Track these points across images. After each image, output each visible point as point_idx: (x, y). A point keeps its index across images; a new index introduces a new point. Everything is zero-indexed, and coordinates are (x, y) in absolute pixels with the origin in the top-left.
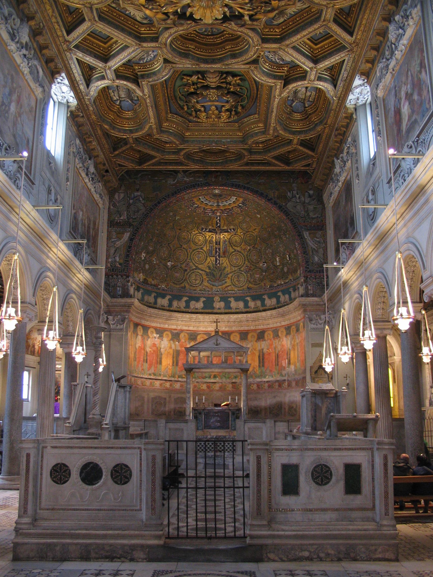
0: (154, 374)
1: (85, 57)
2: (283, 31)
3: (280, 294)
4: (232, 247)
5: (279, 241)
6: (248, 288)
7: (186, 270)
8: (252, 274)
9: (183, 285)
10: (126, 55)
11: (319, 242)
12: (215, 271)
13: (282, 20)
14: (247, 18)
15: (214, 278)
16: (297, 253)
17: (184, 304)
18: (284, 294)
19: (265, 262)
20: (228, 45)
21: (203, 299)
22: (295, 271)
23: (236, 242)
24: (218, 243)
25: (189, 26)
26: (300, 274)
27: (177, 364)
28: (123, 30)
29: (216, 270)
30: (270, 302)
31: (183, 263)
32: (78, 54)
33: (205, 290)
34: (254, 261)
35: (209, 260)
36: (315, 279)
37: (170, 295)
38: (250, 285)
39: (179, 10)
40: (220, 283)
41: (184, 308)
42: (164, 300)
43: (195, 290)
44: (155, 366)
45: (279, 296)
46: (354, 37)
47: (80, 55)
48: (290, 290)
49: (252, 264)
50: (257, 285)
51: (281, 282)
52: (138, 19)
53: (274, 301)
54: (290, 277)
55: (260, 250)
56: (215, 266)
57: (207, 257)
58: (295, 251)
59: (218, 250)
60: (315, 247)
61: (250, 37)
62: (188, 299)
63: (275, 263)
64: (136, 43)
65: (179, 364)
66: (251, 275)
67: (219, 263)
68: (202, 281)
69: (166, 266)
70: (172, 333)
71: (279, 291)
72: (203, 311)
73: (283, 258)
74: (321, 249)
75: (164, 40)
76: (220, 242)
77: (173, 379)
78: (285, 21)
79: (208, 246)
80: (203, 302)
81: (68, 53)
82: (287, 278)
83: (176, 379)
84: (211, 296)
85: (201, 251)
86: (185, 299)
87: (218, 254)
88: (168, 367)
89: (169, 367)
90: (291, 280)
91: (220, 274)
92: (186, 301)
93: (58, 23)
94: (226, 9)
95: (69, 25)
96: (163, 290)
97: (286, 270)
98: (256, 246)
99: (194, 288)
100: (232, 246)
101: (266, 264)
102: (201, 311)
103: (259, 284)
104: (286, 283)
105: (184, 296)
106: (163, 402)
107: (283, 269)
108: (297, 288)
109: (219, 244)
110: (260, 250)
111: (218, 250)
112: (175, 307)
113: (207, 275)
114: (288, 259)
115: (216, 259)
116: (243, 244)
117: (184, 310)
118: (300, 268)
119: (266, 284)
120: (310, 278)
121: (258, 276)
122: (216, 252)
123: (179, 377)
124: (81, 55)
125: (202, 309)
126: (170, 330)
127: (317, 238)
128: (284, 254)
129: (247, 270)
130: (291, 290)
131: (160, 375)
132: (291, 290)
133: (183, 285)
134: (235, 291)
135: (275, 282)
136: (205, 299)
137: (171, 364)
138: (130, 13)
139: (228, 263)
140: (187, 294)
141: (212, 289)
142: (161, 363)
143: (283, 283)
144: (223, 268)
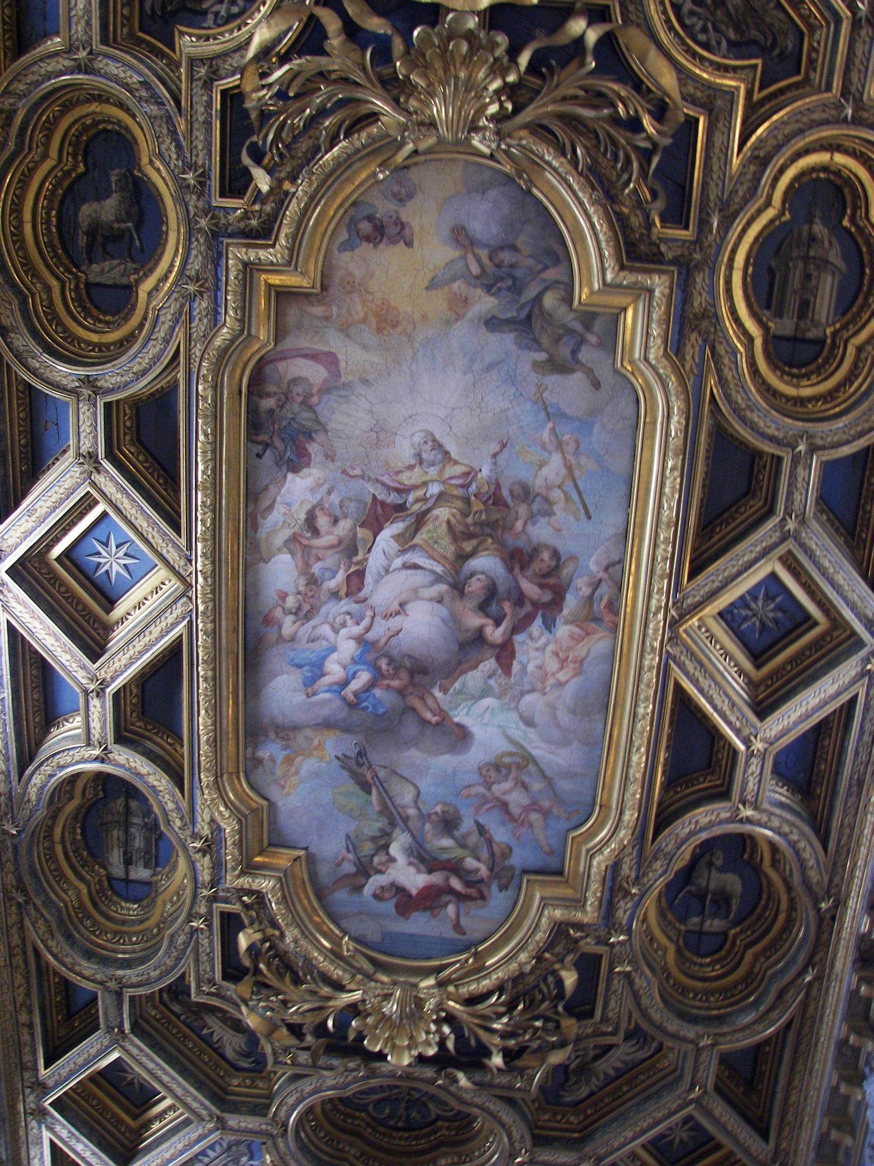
1: (73, 1142)
2: (587, 1121)
10: (180, 1146)
13: (584, 1092)
14: (497, 1060)
20: (445, 1155)
25: (350, 1078)
28: (184, 1072)
32: (58, 1128)
39: (330, 1023)
46: (772, 1143)
47: (64, 1130)
52: (229, 1053)
61: (503, 1125)
64: (211, 1116)
75: (282, 1113)
78: (592, 1094)
81: (34, 1124)
93: (31, 1026)
94: (446, 1029)
95: (57, 1043)
124: (64, 1134)
138: (213, 1032)
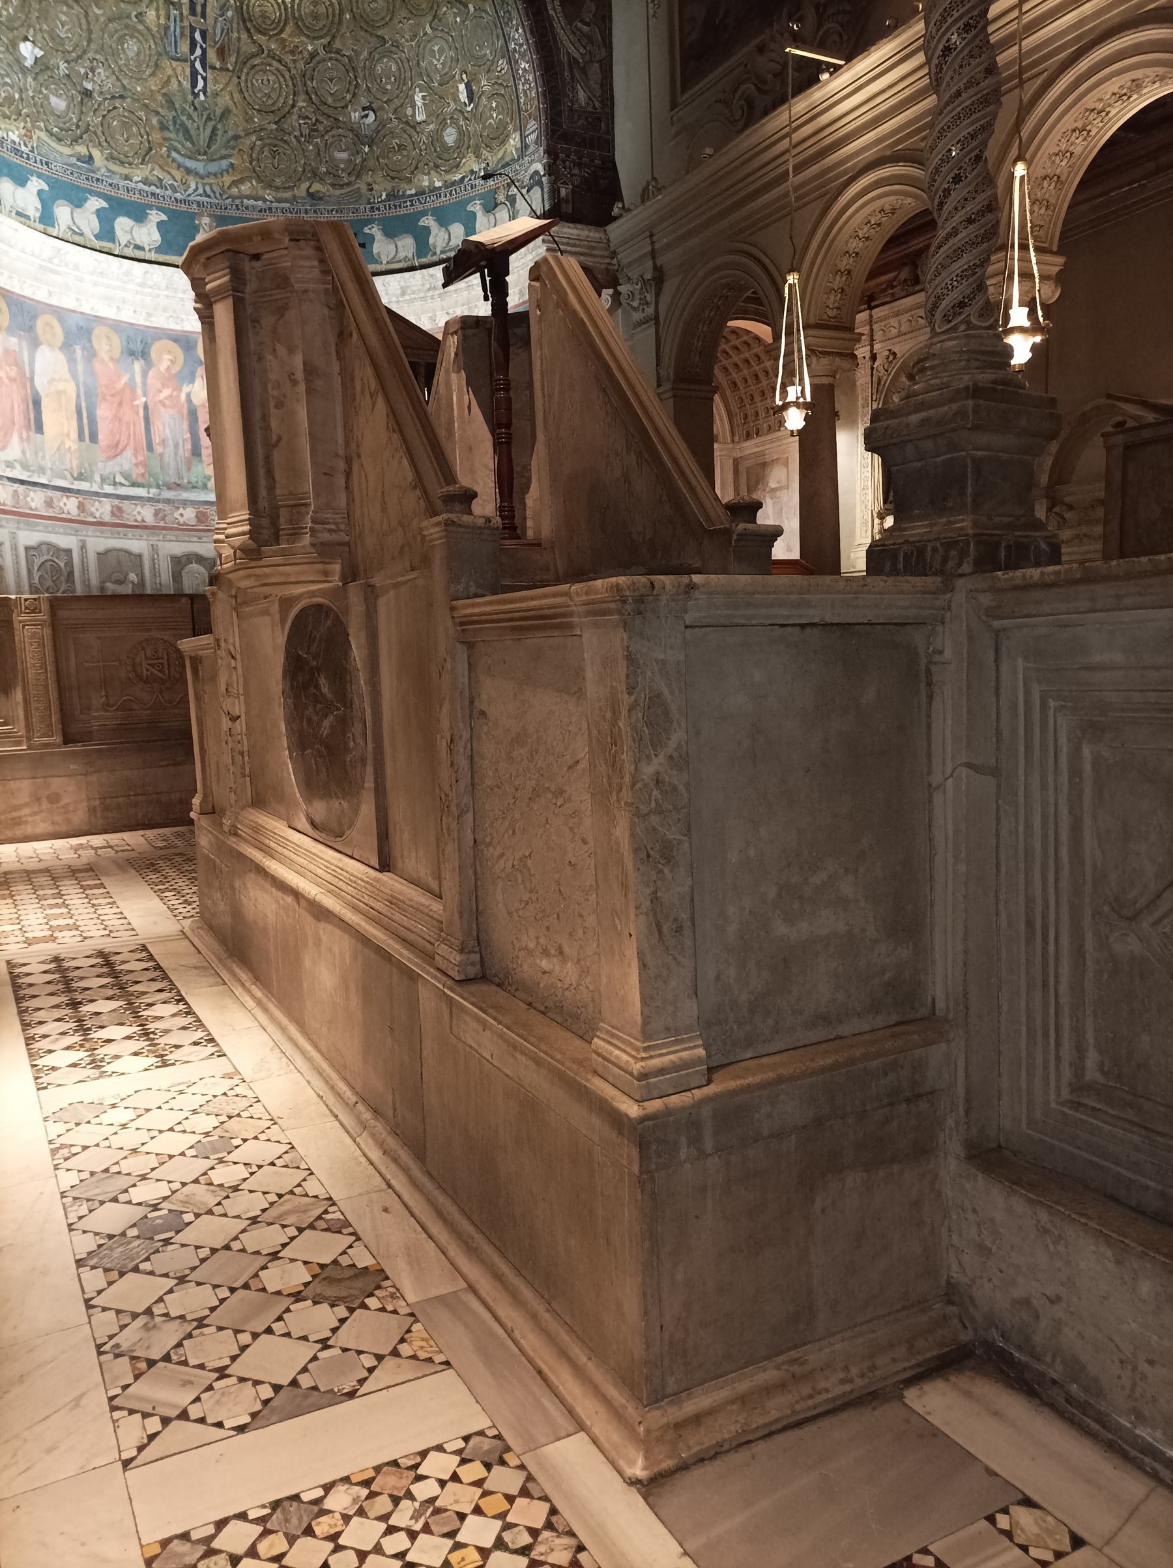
0: (25, 467)
3: (428, 221)
4: (251, 36)
5: (429, 31)
6: (311, 196)
7: (87, 94)
8: (322, 145)
9: (81, 149)
11: (590, 39)
12: (190, 117)
15: (188, 144)
16: (513, 70)
17: (95, 224)
18: (444, 223)
19: (370, 108)
21: (155, 217)
22: (500, 137)
23: (264, 16)
24: (199, 9)
26: (524, 147)
27: (94, 438)
29: (195, 115)
30: (392, 248)
31: (76, 60)
33: (160, 183)
34: (330, 101)
35: (170, 72)
36: (580, 165)
37: (40, 176)
38: (317, 187)
40: (213, 167)
41: (97, 237)
42: (20, 190)
43: (127, 178)
44: (21, 438)
45: (427, 230)
48: (470, 208)
49: (325, 109)
50: (341, 186)
51: (431, 182)
53: (406, 246)
54: (472, 164)
55: (350, 59)
56: (190, 97)
57: (159, 54)
58: (502, 63)
59: (197, 36)
60: (577, 56)
62: (105, 205)
63: (409, 112)
65: (100, 437)
66: (316, 146)
67: (204, 90)
68: (150, 149)
69: (19, 60)
70: (61, 320)
71: (424, 213)
72: (161, 258)
73: (438, 96)
74: (596, 65)
76: (204, 6)
77: (84, 486)
79: (162, 13)
80: (160, 225)
82: (458, 166)
83: (95, 488)
84: (184, 208)
85: (141, 27)
86: (95, 203)
87: (198, 52)
88: (63, 443)
89: (68, 444)
90: (472, 172)
91: (209, 130)
92: (99, 212)
96: (17, 151)
97: (450, 136)
98: (337, 44)
99: (125, 171)
100: (248, 31)
101: (372, 117)
102: (153, 256)
103: (349, 184)
104: (454, 183)
105: (91, 192)
106: (62, 565)
107: (437, 138)
108: (501, 197)
109: (204, 15)
110: (350, 59)
111: (197, 36)
112: (63, 227)
113: (163, 127)
114: (463, 97)
115: (194, 74)
116: (288, 29)
117: (98, 244)
118: (521, 129)
119: (376, 187)
120: (564, 162)
121: (343, 155)
122: (193, 45)
123: (103, 480)
125: (158, 250)
126: (59, 313)
127: (582, 21)
128: (448, 80)
129: (306, 131)
130: (476, 207)
131: (42, 470)
132: (476, 207)
133: (81, 149)
134: (265, 200)
135: (409, 181)
136: (164, 217)
137: (74, 435)
139: (236, 96)
140: (103, 188)
141: (185, 183)
142: (39, 428)
143: (438, 184)
144: (218, 112)
